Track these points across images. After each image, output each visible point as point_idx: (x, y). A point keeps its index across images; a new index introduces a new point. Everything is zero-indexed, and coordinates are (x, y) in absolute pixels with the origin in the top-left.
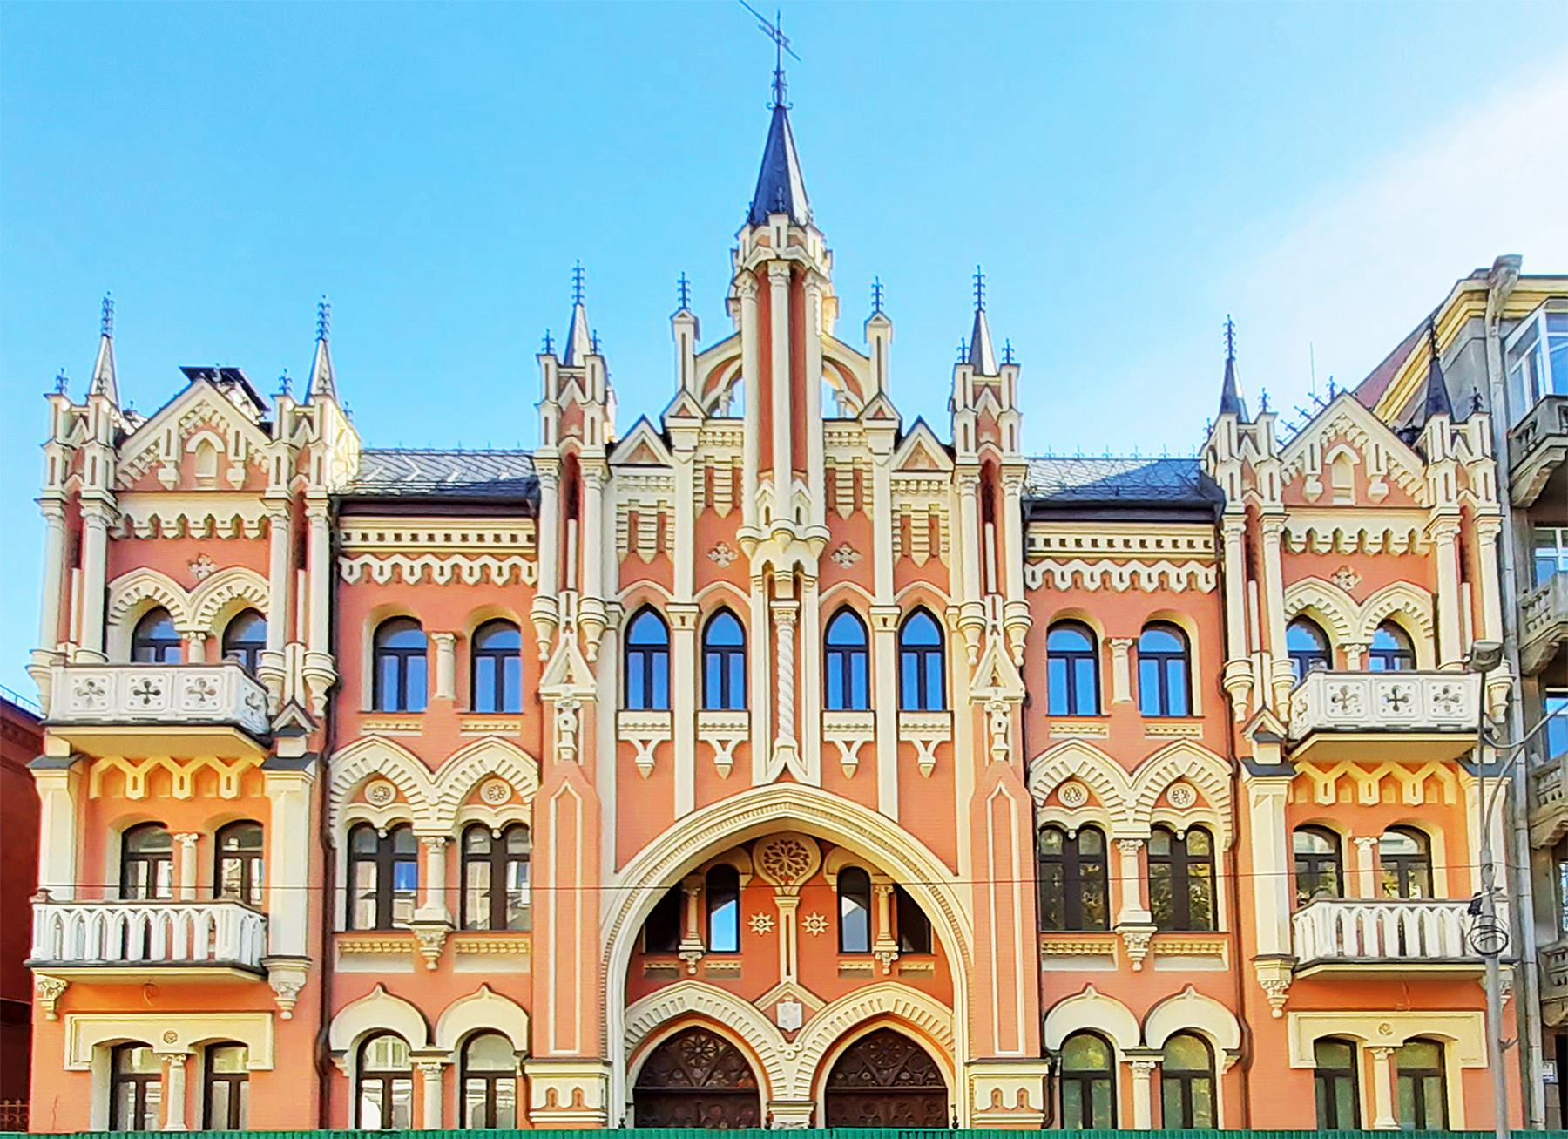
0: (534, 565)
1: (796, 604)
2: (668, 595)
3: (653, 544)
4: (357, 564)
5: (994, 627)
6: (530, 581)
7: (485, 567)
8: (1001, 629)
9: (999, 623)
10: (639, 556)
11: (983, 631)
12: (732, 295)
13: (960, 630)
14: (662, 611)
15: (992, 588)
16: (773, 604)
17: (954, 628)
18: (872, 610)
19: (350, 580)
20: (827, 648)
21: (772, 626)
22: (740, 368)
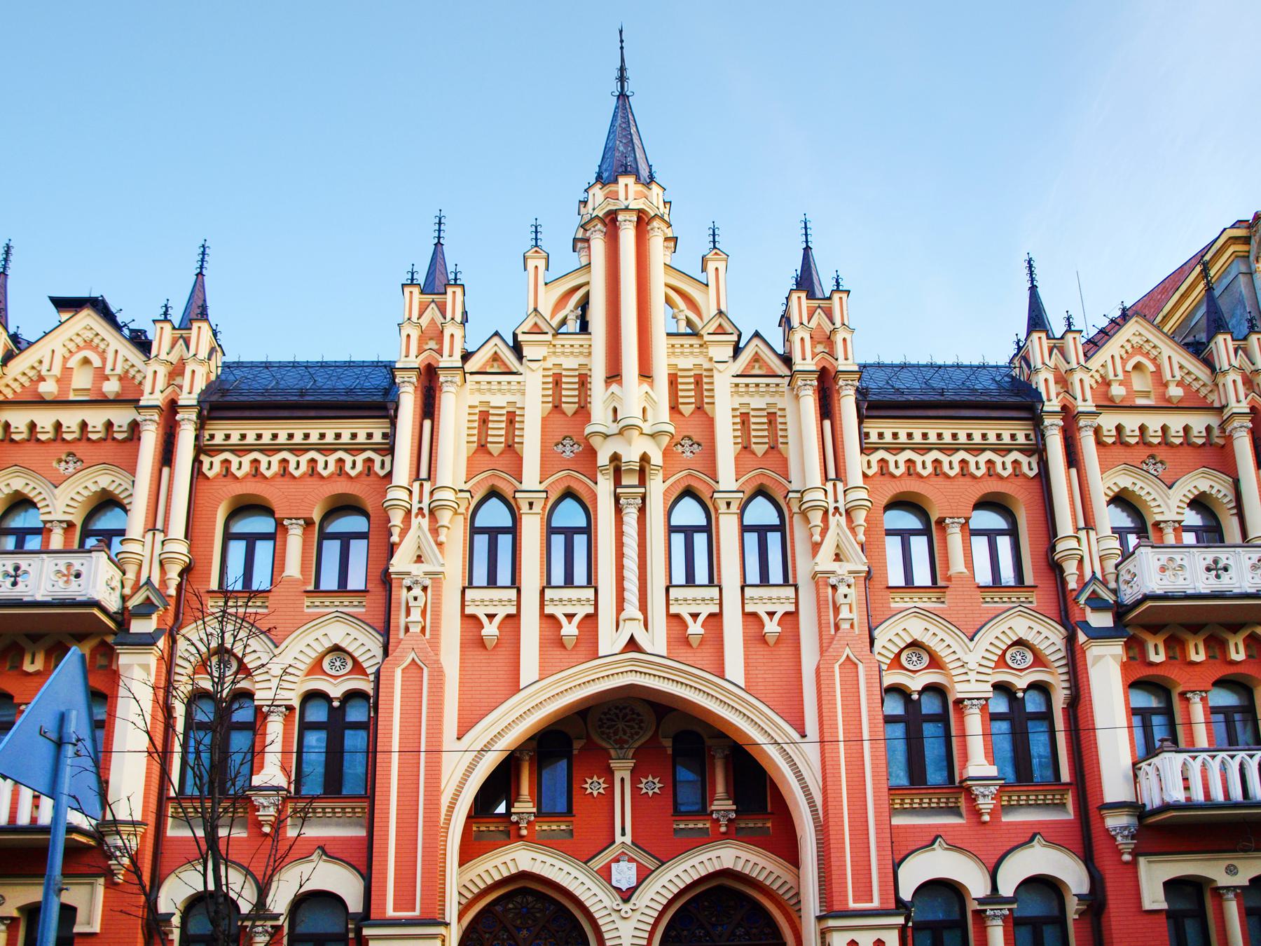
0: (388, 459)
1: (642, 490)
2: (516, 483)
3: (502, 439)
4: (217, 460)
5: (836, 509)
6: (382, 473)
7: (341, 461)
8: (842, 510)
9: (841, 505)
10: (496, 448)
11: (826, 512)
12: (580, 235)
13: (804, 514)
14: (509, 496)
15: (832, 474)
16: (619, 490)
17: (796, 509)
18: (716, 495)
19: (210, 474)
20: (672, 529)
21: (619, 510)
22: (587, 295)
